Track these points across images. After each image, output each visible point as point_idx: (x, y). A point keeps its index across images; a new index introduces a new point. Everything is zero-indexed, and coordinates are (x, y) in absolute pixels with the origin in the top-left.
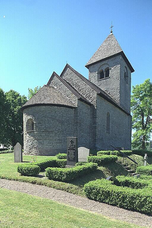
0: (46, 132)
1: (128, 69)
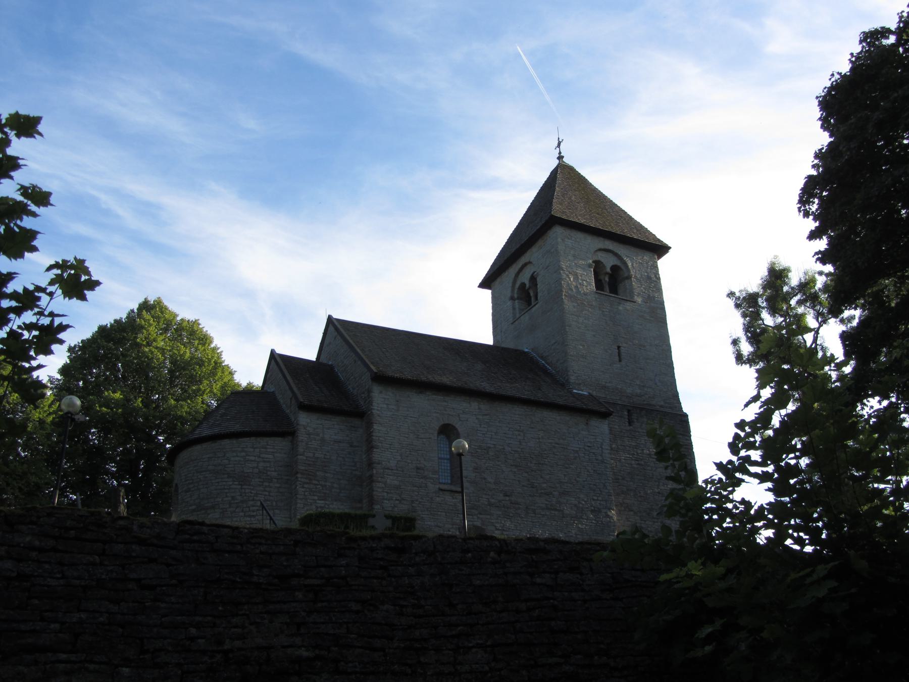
1: (622, 250)
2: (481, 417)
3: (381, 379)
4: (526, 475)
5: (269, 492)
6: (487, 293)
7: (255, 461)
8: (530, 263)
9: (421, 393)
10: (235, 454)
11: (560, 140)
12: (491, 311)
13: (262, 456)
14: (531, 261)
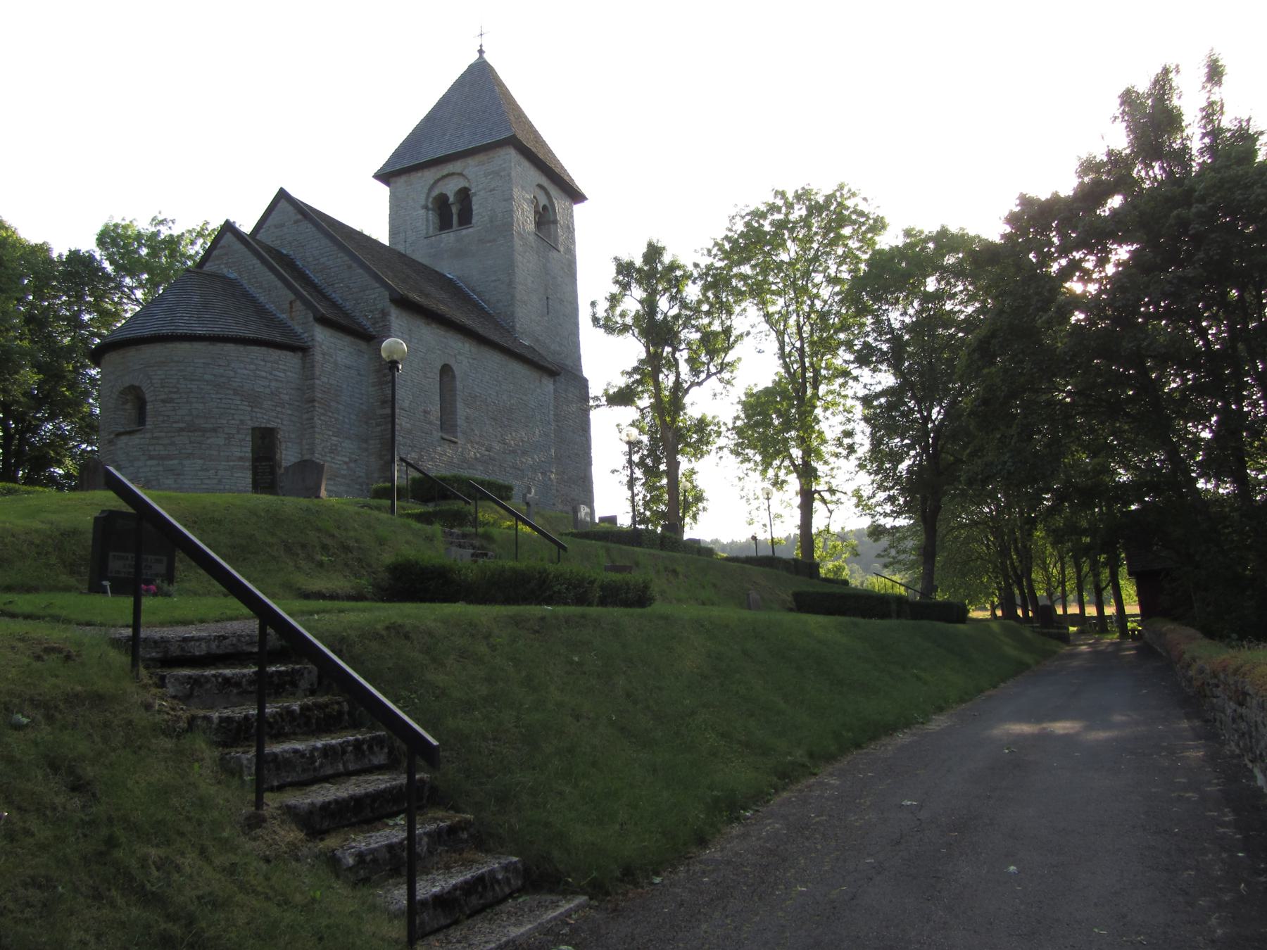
0: (191, 432)
1: (554, 191)
2: (470, 360)
3: (404, 304)
4: (500, 429)
5: (282, 419)
6: (384, 191)
7: (266, 378)
8: (461, 174)
9: (428, 324)
10: (242, 365)
11: (484, 31)
12: (388, 212)
13: (274, 372)
14: (464, 173)
